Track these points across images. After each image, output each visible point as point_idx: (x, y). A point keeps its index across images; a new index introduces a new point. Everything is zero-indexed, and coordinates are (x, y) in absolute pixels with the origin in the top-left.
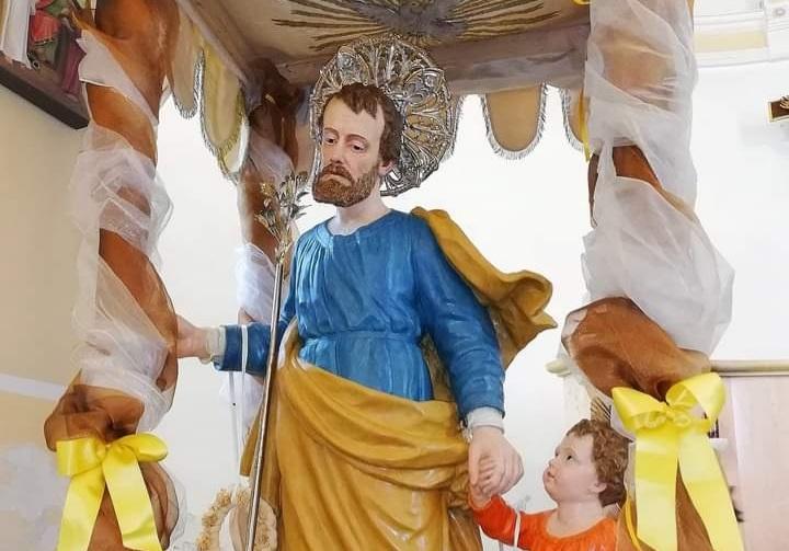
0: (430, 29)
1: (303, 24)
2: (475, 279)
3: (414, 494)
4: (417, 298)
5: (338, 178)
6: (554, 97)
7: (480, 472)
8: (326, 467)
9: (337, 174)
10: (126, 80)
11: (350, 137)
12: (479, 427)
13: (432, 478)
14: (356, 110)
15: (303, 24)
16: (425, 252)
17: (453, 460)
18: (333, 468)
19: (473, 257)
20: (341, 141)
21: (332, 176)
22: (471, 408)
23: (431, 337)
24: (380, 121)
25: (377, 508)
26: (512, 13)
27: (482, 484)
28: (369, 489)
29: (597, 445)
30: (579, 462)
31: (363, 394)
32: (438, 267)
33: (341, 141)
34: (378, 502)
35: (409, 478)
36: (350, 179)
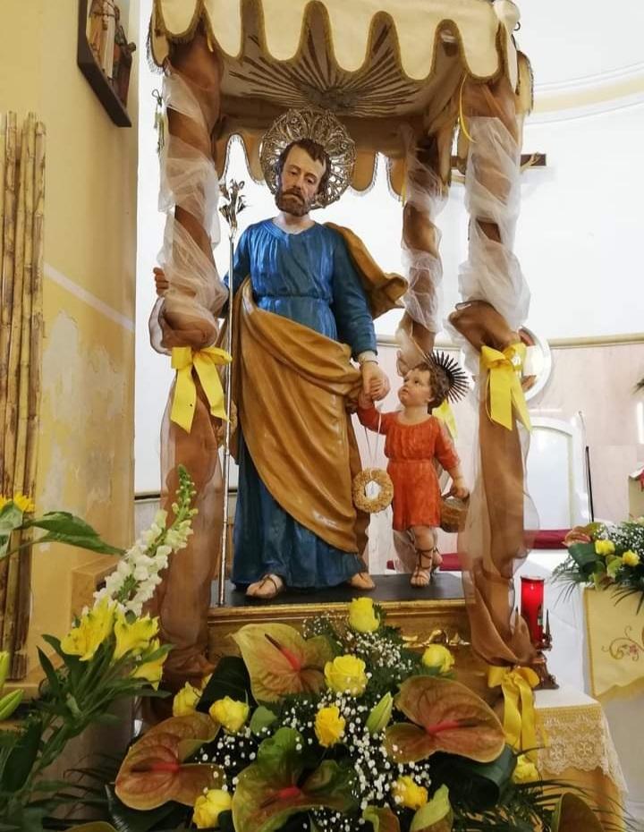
0: (335, 107)
1: (253, 81)
2: (369, 274)
3: (334, 397)
4: (333, 280)
5: (296, 198)
6: (382, 160)
7: (372, 387)
8: (286, 380)
9: (297, 195)
10: (199, 110)
11: (308, 174)
12: (368, 361)
13: (342, 389)
14: (314, 159)
15: (253, 81)
16: (341, 253)
17: (353, 379)
18: (290, 380)
19: (369, 262)
20: (302, 176)
21: (293, 196)
22: (362, 352)
23: (338, 308)
24: (323, 169)
25: (317, 403)
26: (267, 79)
27: (373, 393)
28: (312, 391)
29: (432, 376)
30: (422, 385)
31: (313, 335)
32: (346, 261)
33: (302, 176)
34: (318, 400)
35: (334, 387)
36: (304, 201)
